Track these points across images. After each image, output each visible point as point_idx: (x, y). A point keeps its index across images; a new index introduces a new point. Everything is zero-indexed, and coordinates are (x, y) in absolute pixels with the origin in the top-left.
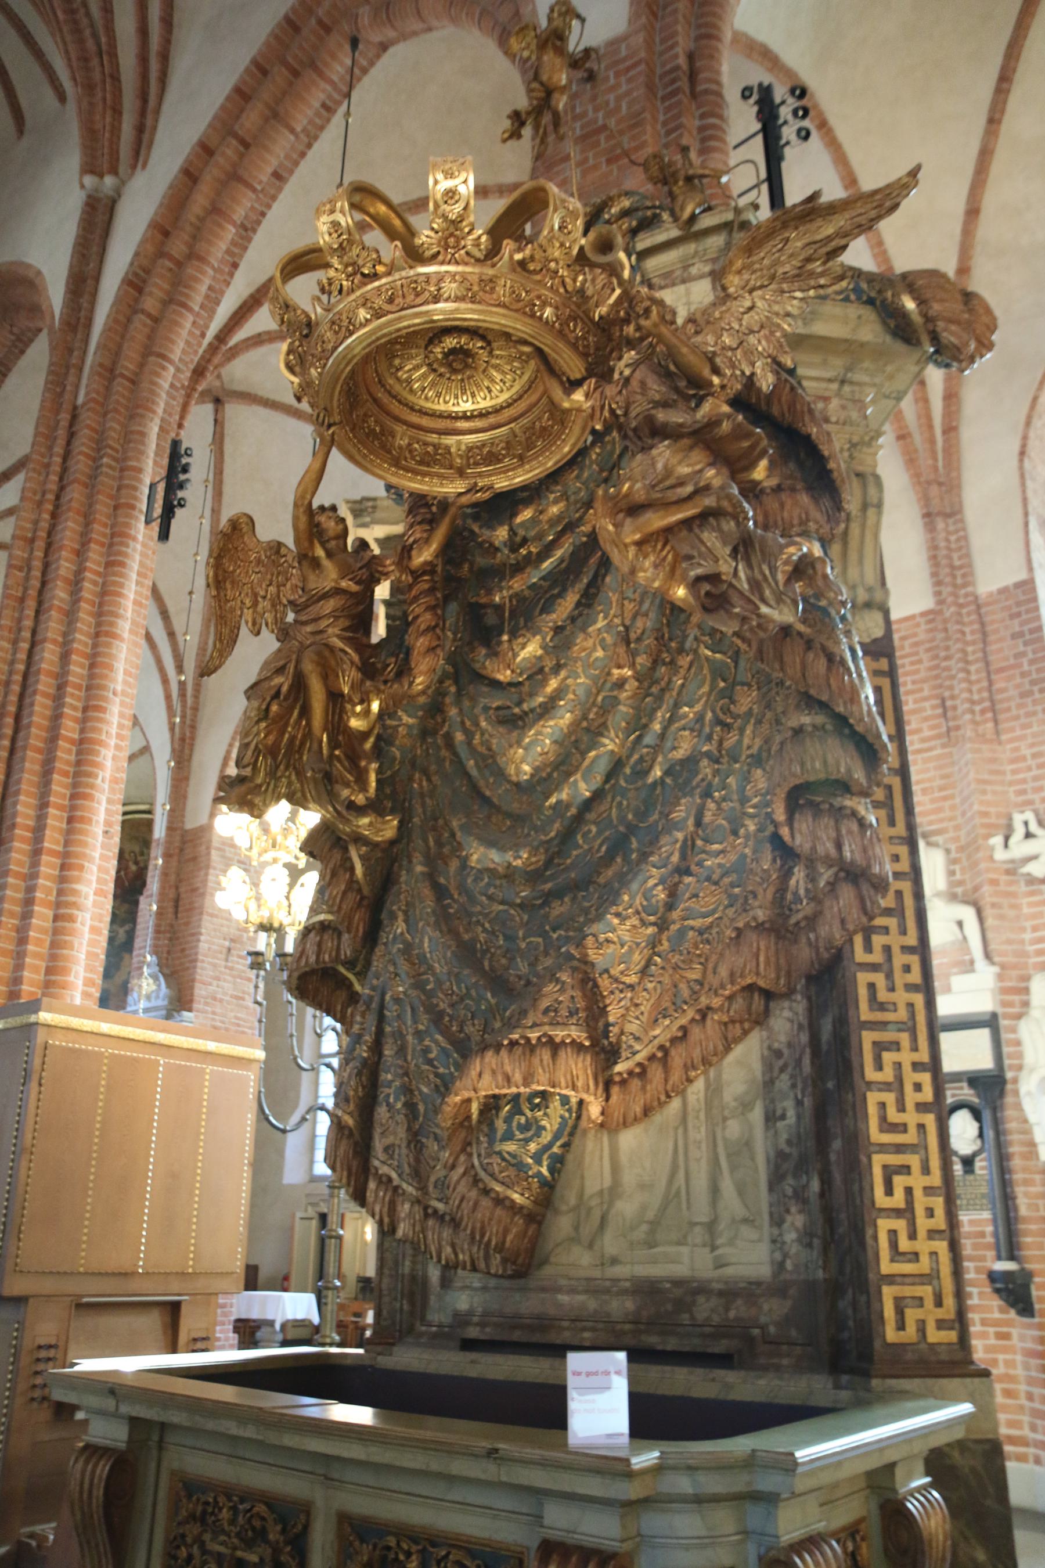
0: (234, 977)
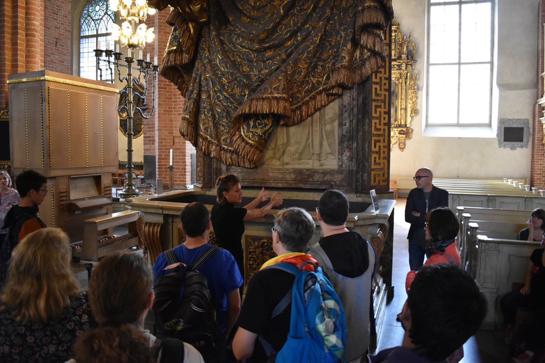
0: (59, 53)
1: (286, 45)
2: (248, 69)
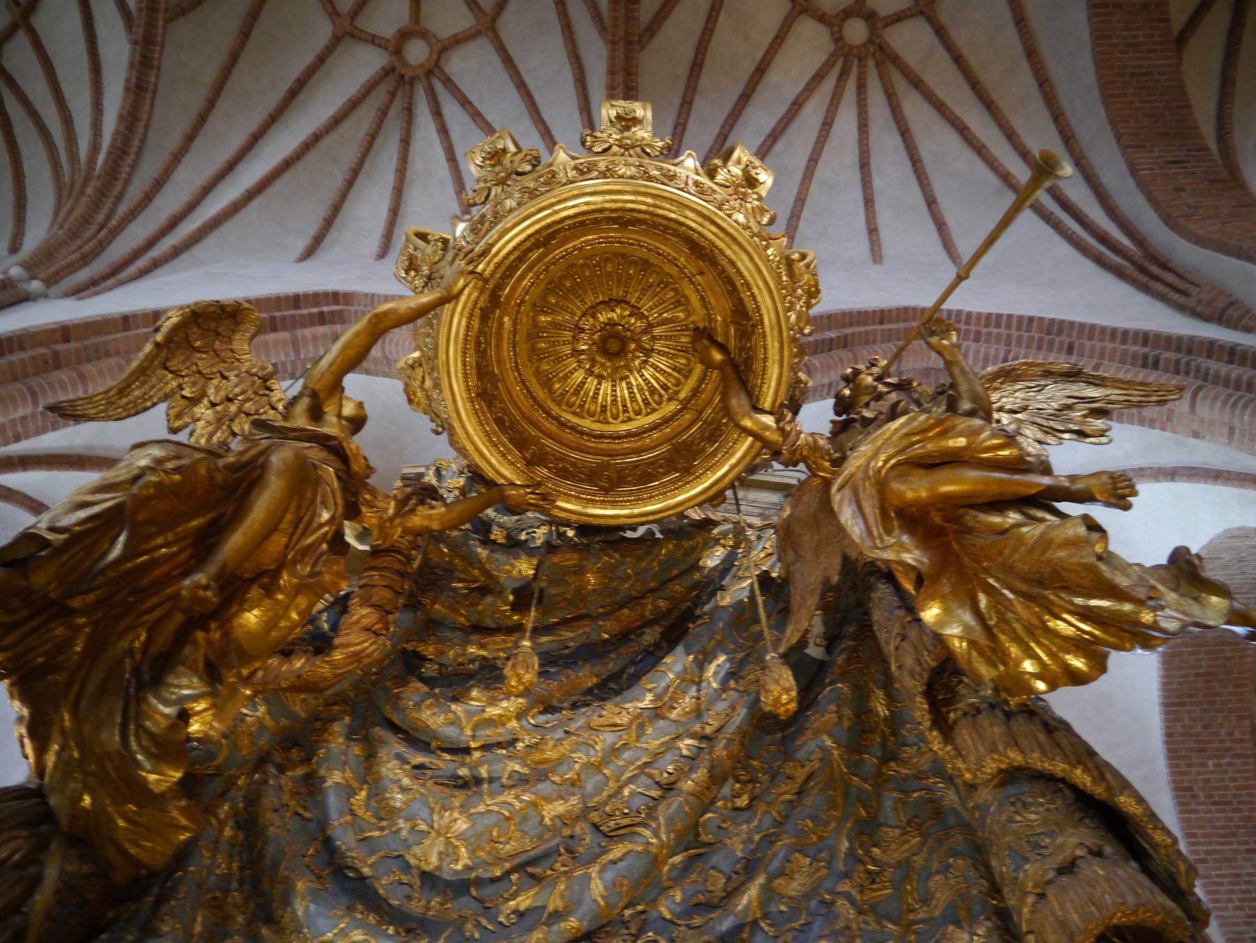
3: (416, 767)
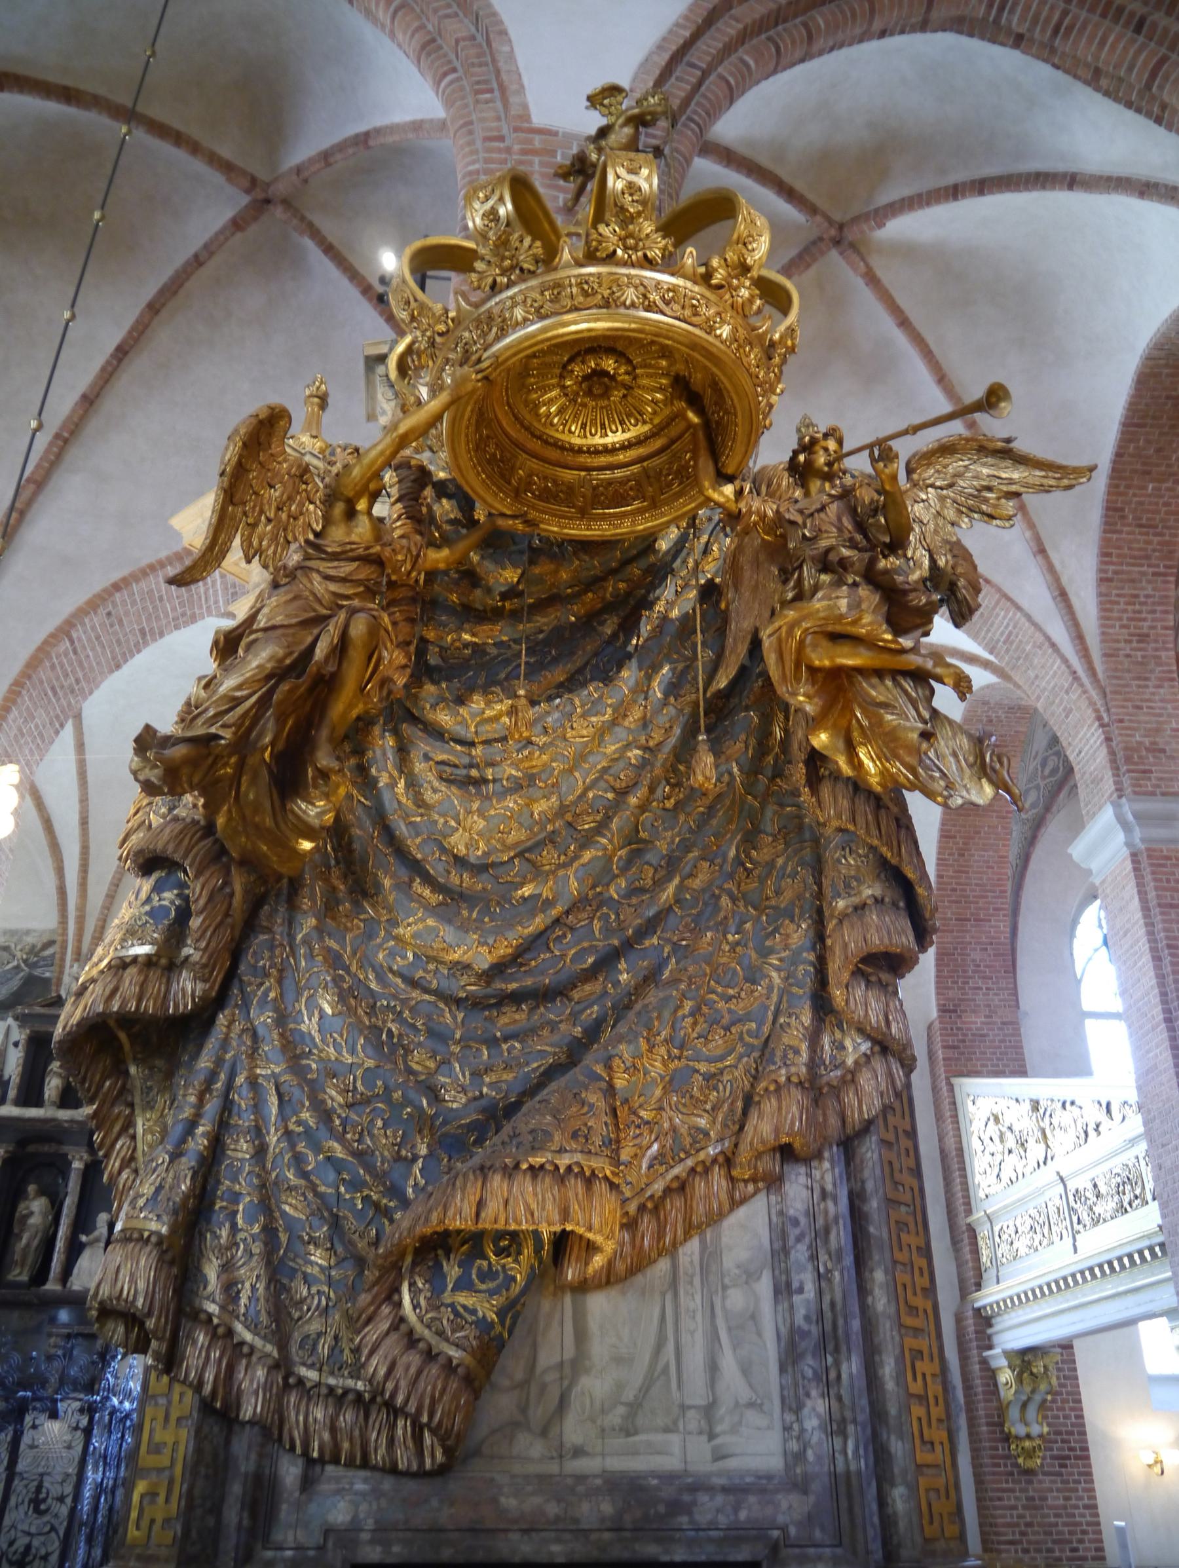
1: (576, 995)
2: (431, 1064)
3: (437, 763)
